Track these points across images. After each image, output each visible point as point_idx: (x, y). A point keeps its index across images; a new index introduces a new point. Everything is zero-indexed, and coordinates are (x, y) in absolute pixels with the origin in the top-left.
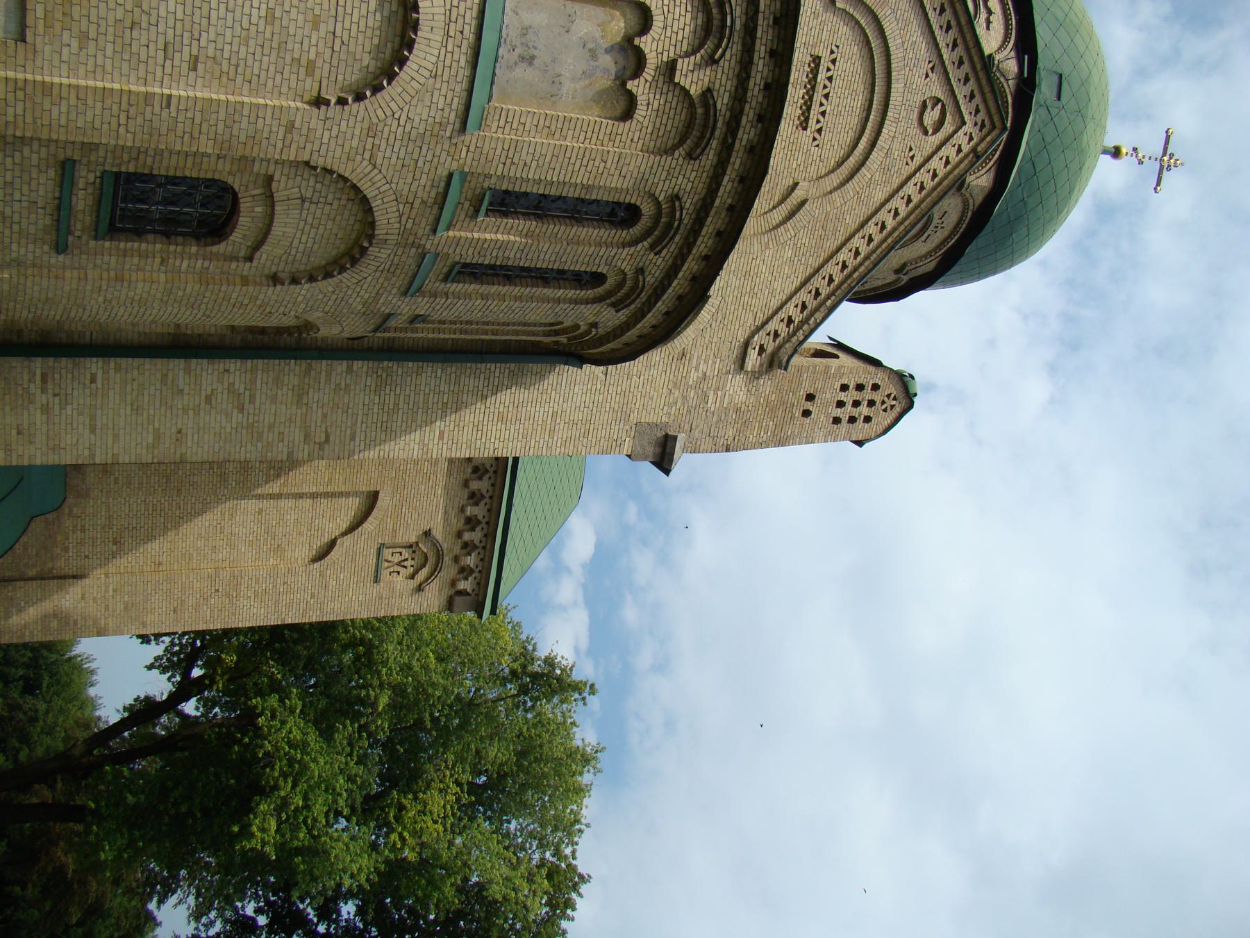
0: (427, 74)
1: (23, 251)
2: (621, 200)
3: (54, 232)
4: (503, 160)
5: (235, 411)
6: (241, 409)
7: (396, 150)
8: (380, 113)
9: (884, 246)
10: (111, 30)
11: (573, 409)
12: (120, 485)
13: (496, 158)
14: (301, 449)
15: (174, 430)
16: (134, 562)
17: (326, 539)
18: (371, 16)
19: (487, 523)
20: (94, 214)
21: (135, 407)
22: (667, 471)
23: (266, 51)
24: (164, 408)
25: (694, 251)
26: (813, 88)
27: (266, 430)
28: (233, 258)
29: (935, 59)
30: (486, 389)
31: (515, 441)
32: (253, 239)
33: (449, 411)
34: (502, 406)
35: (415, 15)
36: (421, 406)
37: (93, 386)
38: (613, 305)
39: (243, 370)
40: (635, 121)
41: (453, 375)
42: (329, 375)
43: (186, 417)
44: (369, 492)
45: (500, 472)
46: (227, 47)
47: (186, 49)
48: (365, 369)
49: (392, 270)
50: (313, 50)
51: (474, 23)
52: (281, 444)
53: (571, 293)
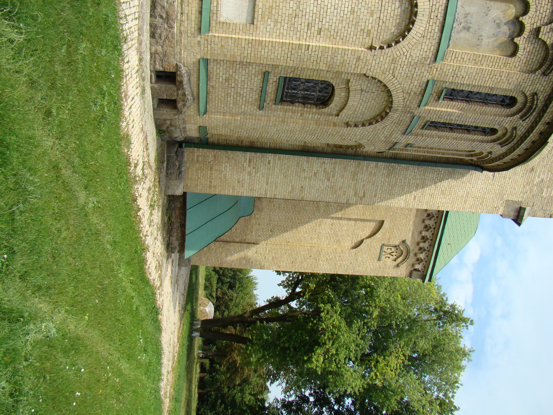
0: (420, 35)
1: (246, 108)
2: (508, 95)
3: (259, 101)
4: (452, 75)
5: (326, 180)
6: (329, 180)
7: (404, 69)
8: (398, 53)
10: (287, 18)
11: (476, 191)
13: (450, 74)
14: (352, 199)
15: (300, 186)
17: (359, 239)
18: (396, 10)
19: (431, 240)
20: (275, 94)
21: (285, 175)
22: (519, 224)
23: (350, 26)
24: (296, 176)
25: (542, 120)
28: (330, 115)
30: (437, 179)
31: (448, 204)
33: (419, 187)
34: (443, 187)
35: (416, 9)
36: (407, 184)
38: (500, 144)
39: (331, 163)
40: (517, 57)
41: (422, 172)
42: (367, 167)
44: (380, 221)
45: (439, 217)
46: (334, 25)
47: (317, 26)
48: (383, 166)
49: (399, 123)
50: (370, 25)
51: (443, 12)
52: (344, 196)
53: (480, 137)
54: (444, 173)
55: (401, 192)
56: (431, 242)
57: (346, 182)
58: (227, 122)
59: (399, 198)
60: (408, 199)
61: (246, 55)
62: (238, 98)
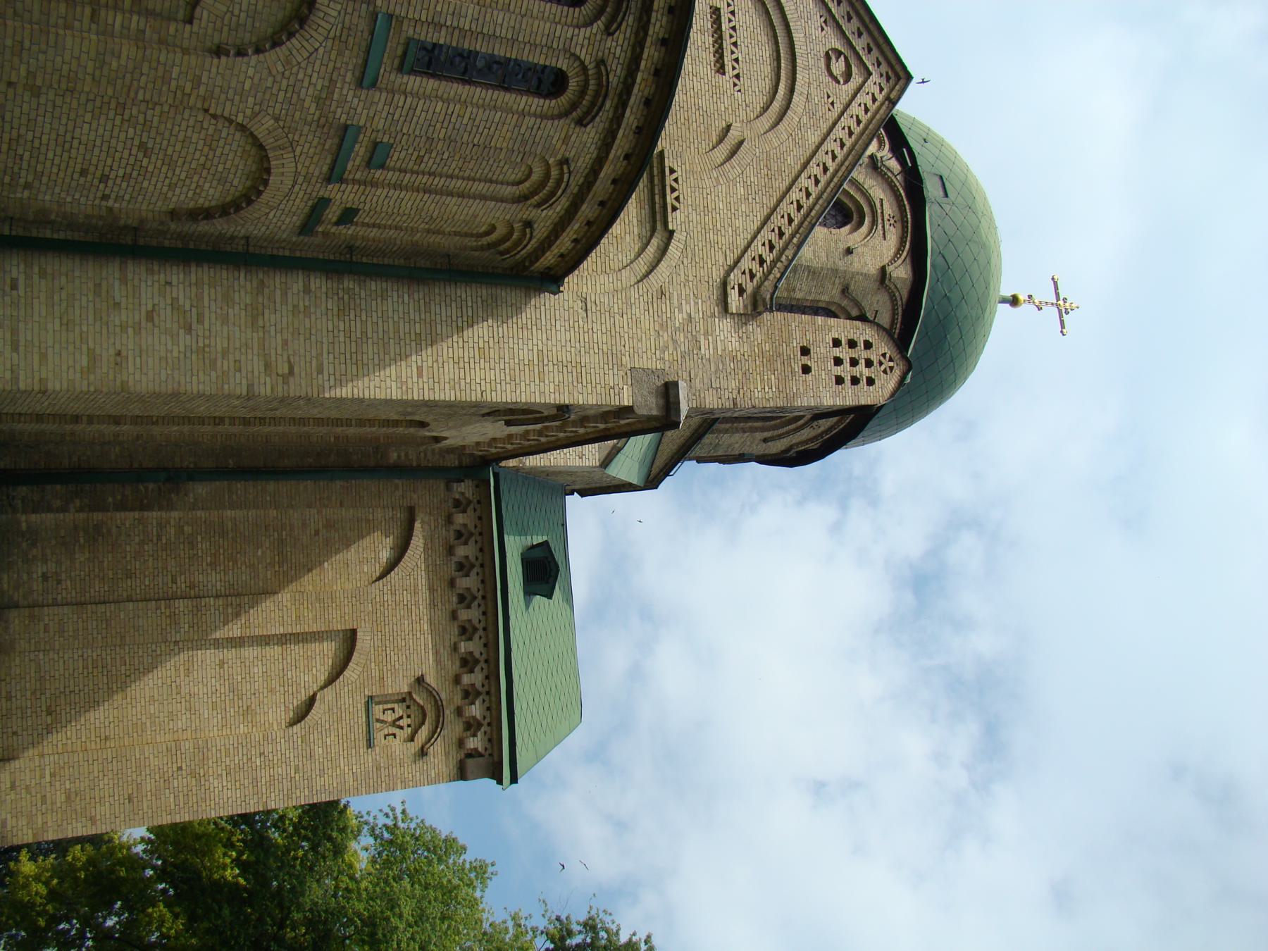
5: (182, 331)
6: (189, 329)
9: (832, 185)
11: (559, 349)
12: (52, 634)
15: (112, 352)
16: (74, 737)
17: (303, 696)
19: (486, 661)
21: (65, 321)
24: (98, 324)
25: (651, 32)
26: (721, 37)
27: (219, 356)
29: (824, 12)
30: (460, 319)
31: (503, 383)
33: (423, 343)
36: (392, 336)
37: (14, 292)
39: (187, 283)
41: (422, 301)
42: (284, 294)
43: (125, 336)
45: (489, 596)
48: (324, 289)
52: (238, 375)
53: (536, 103)
54: (474, 305)
55: (382, 356)
56: (489, 667)
57: (237, 335)
59: (382, 373)
60: (404, 375)
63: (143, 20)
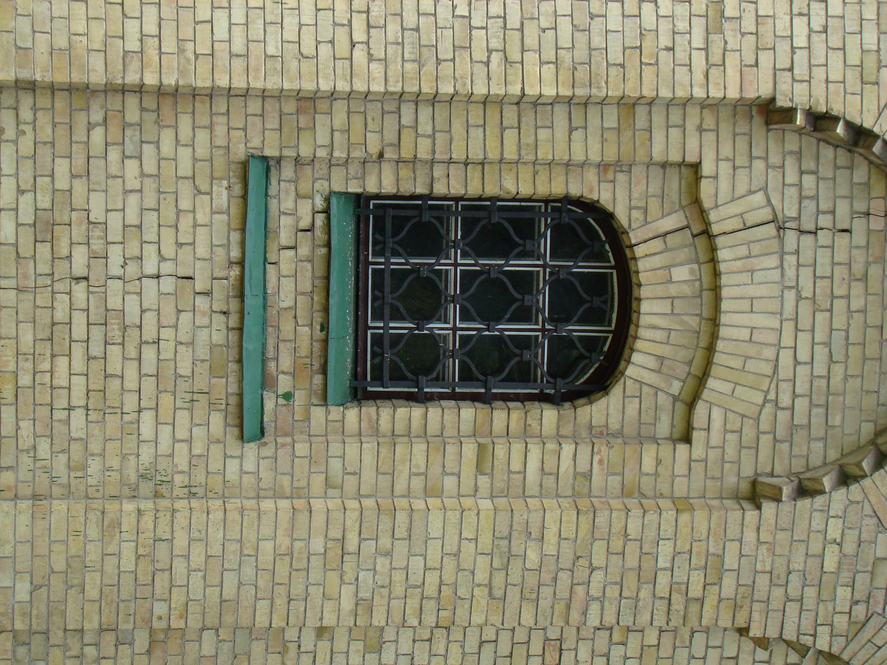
3: (233, 367)
20: (318, 318)
32: (682, 370)
58: (59, 564)
61: (133, 45)
62: (114, 351)
63: (584, 452)
